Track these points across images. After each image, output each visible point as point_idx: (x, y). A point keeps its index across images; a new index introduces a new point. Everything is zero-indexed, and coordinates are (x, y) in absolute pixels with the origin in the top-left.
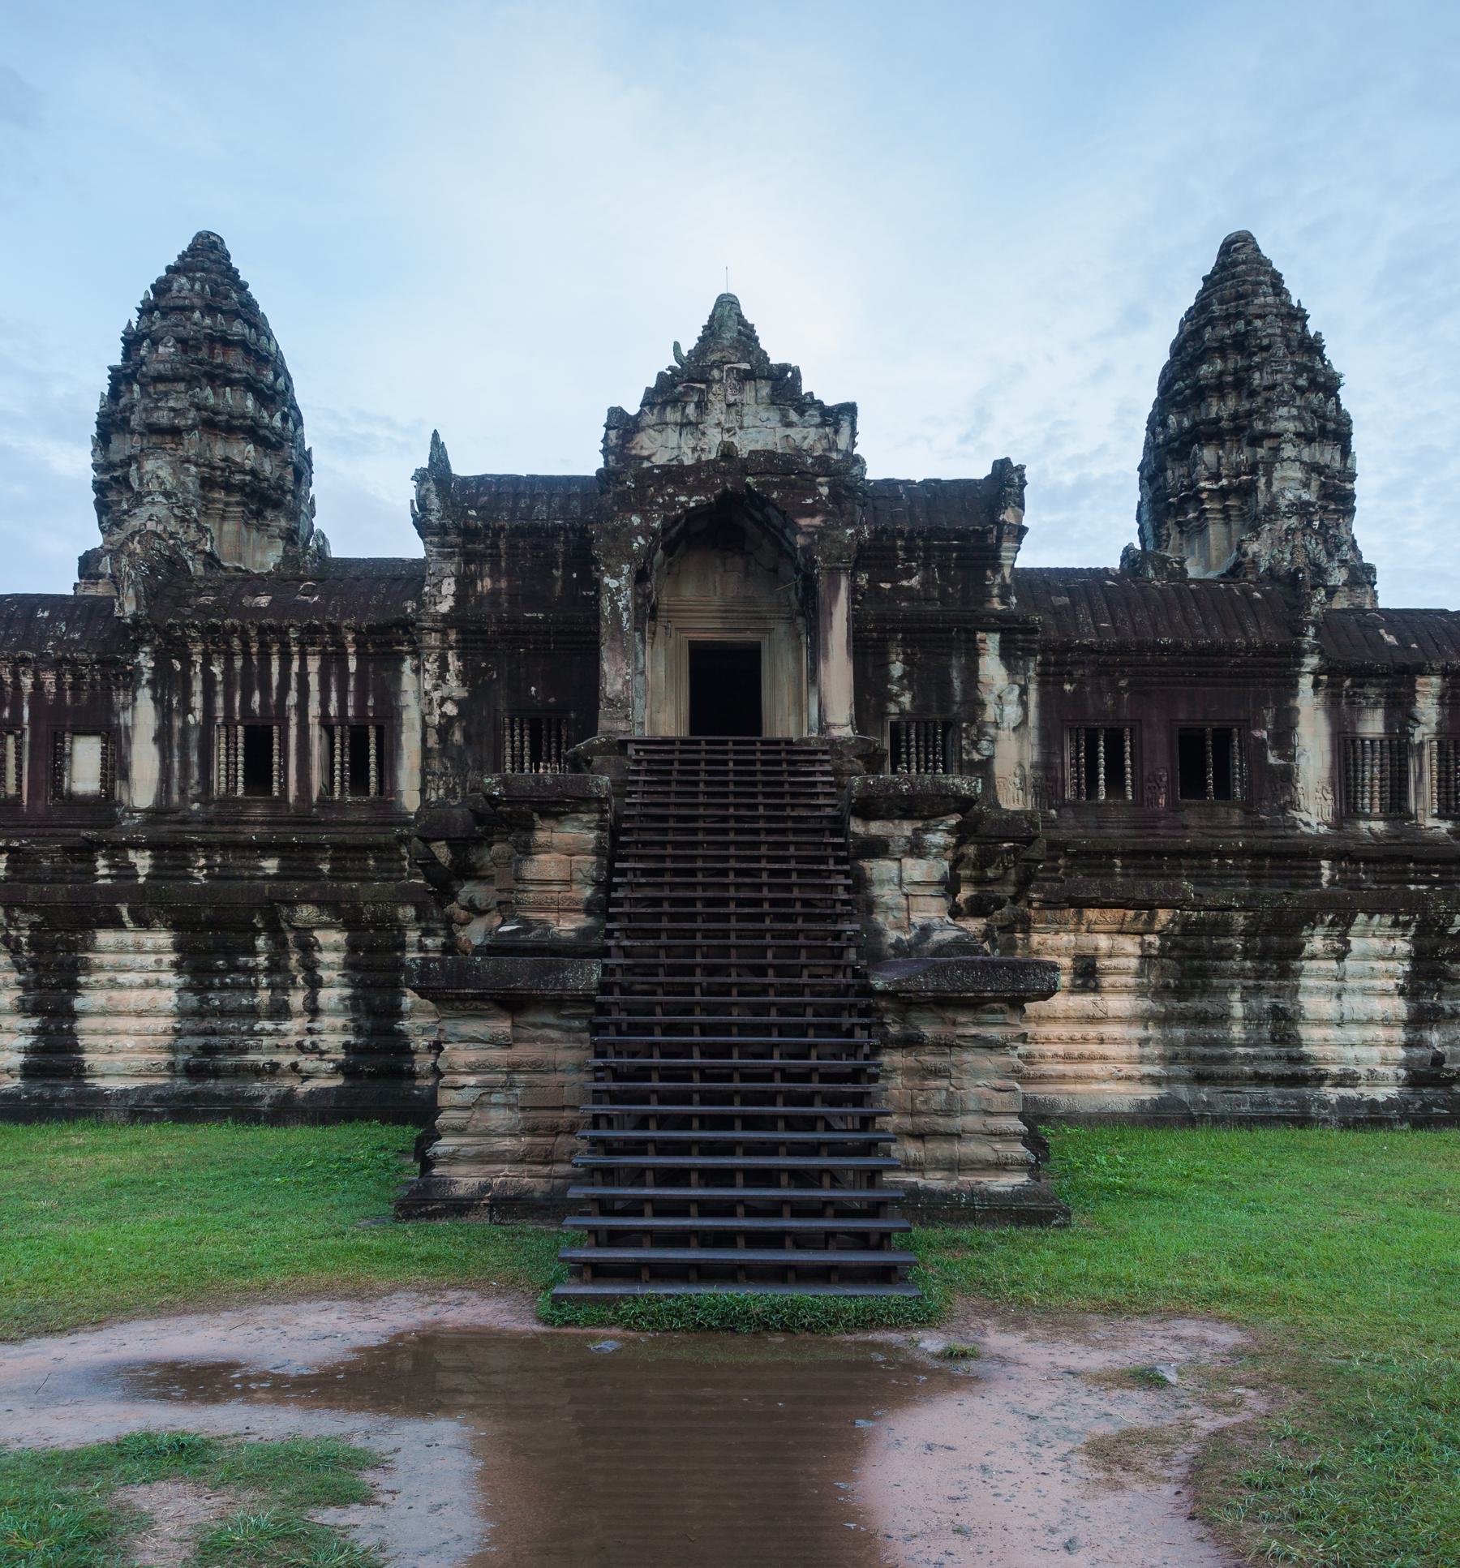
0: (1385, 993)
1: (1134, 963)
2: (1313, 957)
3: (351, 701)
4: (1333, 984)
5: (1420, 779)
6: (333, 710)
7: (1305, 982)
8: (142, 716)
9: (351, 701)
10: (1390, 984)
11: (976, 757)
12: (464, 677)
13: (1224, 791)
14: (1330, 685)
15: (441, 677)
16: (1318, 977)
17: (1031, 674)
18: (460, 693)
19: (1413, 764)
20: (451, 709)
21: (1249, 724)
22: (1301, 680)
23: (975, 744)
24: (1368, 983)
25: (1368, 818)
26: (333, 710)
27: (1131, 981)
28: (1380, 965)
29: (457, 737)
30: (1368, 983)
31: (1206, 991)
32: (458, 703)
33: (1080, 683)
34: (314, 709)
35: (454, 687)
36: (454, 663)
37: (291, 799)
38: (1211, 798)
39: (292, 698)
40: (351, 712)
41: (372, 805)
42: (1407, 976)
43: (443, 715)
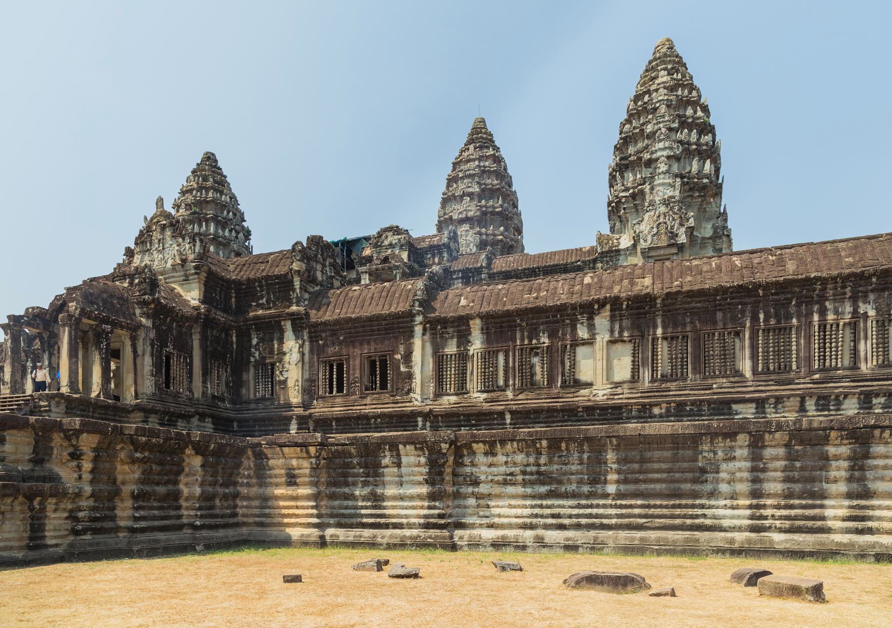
0: (420, 483)
1: (307, 471)
2: (387, 467)
4: (397, 479)
5: (472, 373)
7: (387, 479)
10: (420, 478)
11: (282, 378)
13: (384, 386)
14: (431, 329)
16: (391, 476)
17: (305, 338)
19: (469, 365)
21: (394, 351)
22: (471, 322)
23: (281, 372)
24: (412, 478)
25: (449, 395)
27: (307, 479)
28: (417, 469)
30: (412, 478)
31: (347, 484)
33: (326, 340)
38: (378, 390)
42: (429, 473)
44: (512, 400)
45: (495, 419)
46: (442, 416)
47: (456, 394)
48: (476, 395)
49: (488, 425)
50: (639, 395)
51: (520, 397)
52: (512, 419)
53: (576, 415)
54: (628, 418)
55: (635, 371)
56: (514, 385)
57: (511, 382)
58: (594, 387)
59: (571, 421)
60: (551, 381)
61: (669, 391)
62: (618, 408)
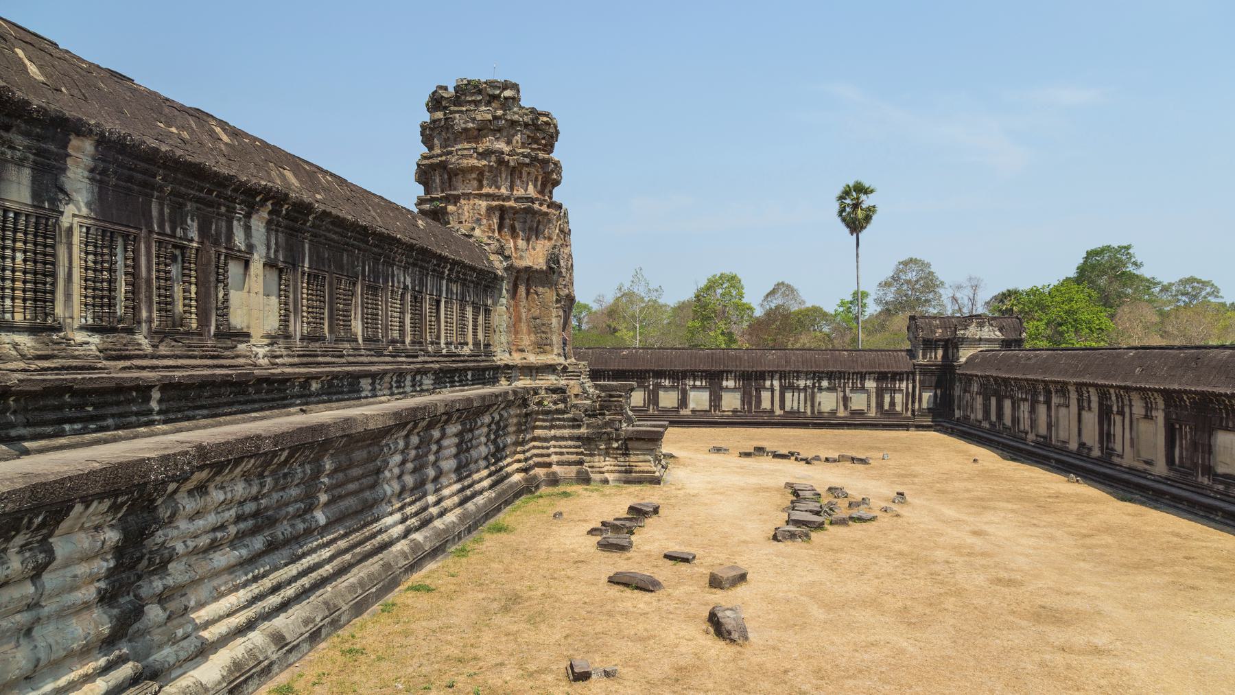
44: (153, 357)
45: (133, 401)
46: (20, 395)
47: (33, 330)
48: (80, 337)
49: (121, 415)
50: (296, 360)
51: (163, 349)
52: (160, 402)
53: (244, 393)
54: (292, 397)
55: (285, 320)
56: (150, 320)
57: (144, 314)
58: (253, 341)
59: (240, 403)
60: (204, 320)
61: (317, 356)
62: (285, 381)
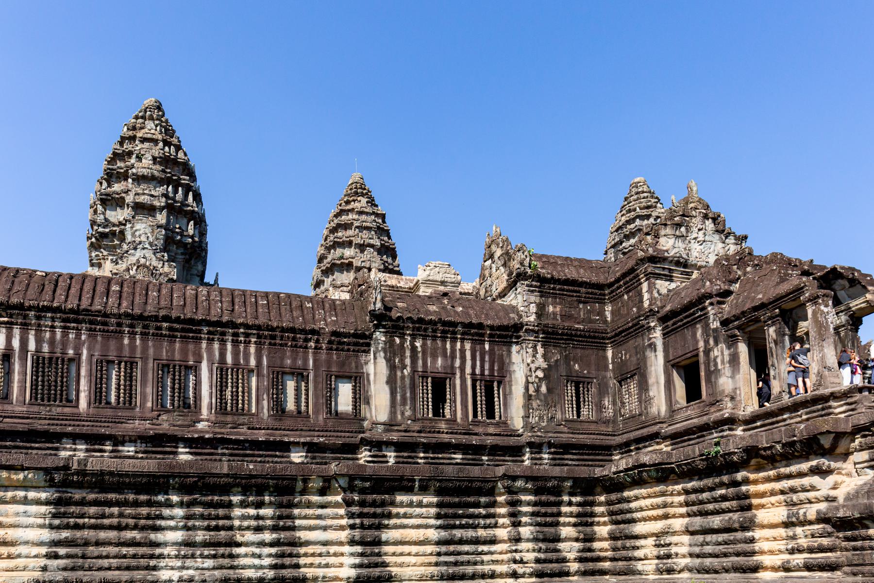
3: (487, 366)
6: (478, 371)
8: (376, 368)
9: (487, 366)
12: (544, 356)
15: (534, 356)
18: (544, 365)
20: (540, 374)
26: (478, 371)
29: (544, 389)
32: (544, 370)
34: (468, 370)
35: (541, 362)
36: (540, 350)
37: (459, 420)
39: (457, 363)
40: (487, 373)
41: (497, 424)
43: (537, 377)
